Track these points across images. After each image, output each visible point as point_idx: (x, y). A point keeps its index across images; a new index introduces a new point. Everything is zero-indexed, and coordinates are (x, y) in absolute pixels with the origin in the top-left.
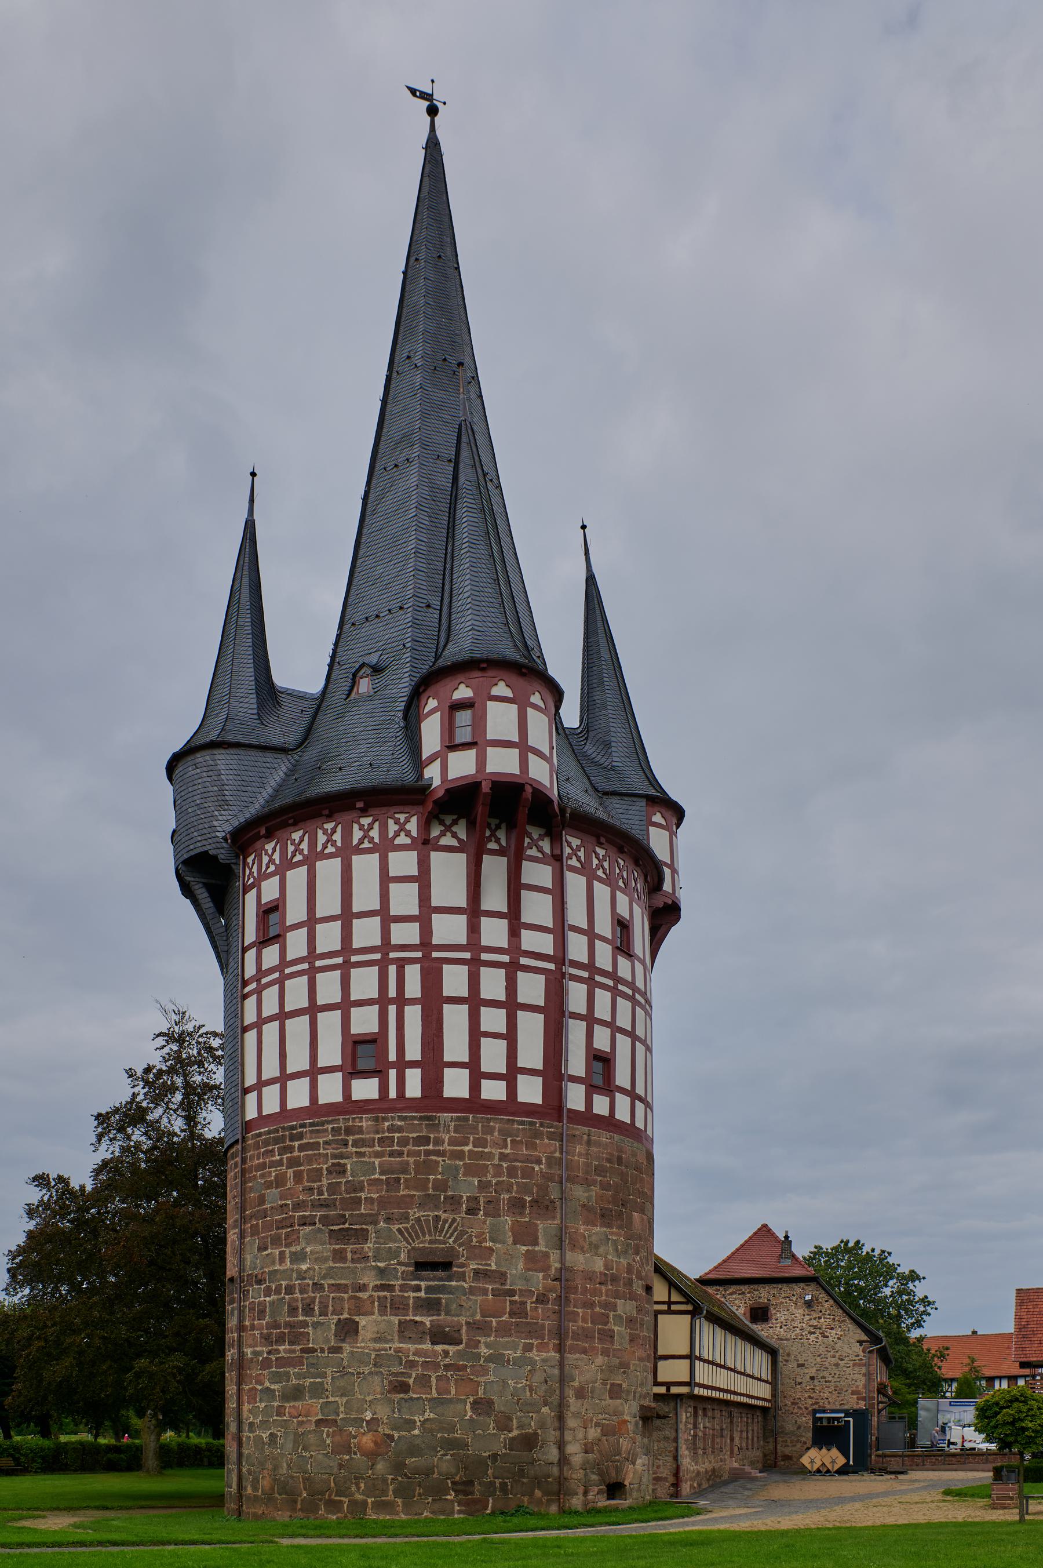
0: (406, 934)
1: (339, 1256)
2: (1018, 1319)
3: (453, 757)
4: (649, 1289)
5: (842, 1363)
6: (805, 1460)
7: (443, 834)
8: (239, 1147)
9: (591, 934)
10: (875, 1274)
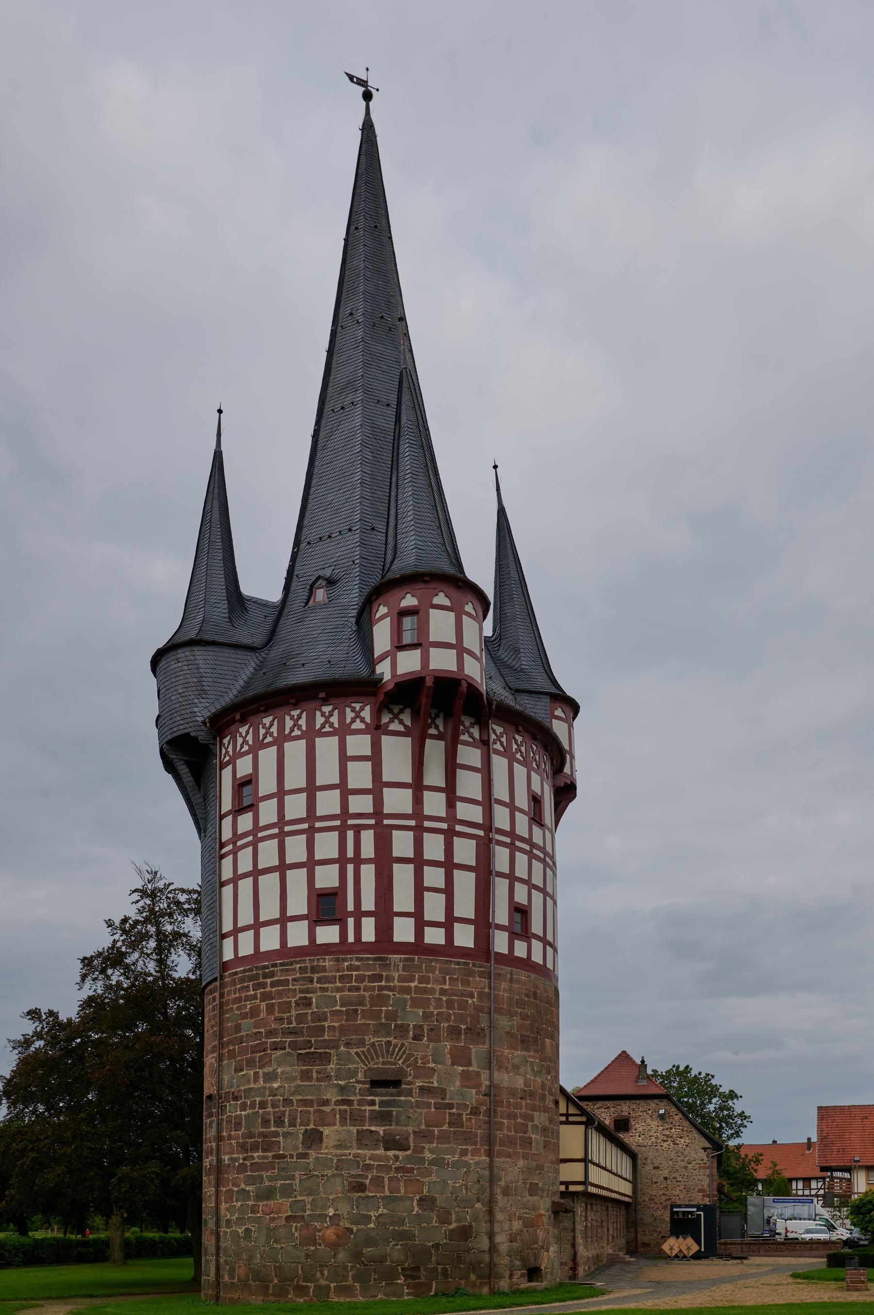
0: (361, 804)
1: (306, 1075)
2: (820, 1131)
3: (401, 655)
4: (557, 1103)
5: (690, 1166)
6: (666, 1247)
7: (391, 721)
8: (218, 983)
9: (513, 808)
10: (701, 1093)
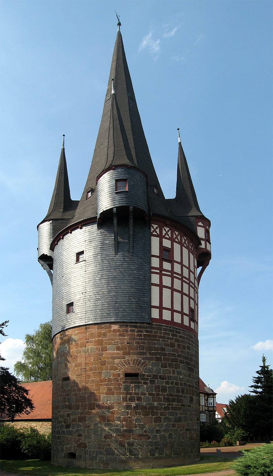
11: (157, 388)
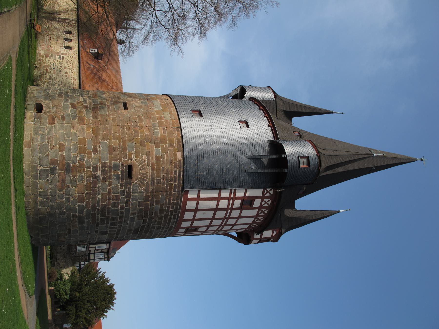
1: (130, 230)
11: (117, 198)
